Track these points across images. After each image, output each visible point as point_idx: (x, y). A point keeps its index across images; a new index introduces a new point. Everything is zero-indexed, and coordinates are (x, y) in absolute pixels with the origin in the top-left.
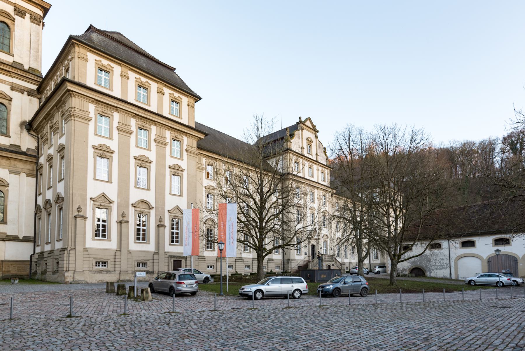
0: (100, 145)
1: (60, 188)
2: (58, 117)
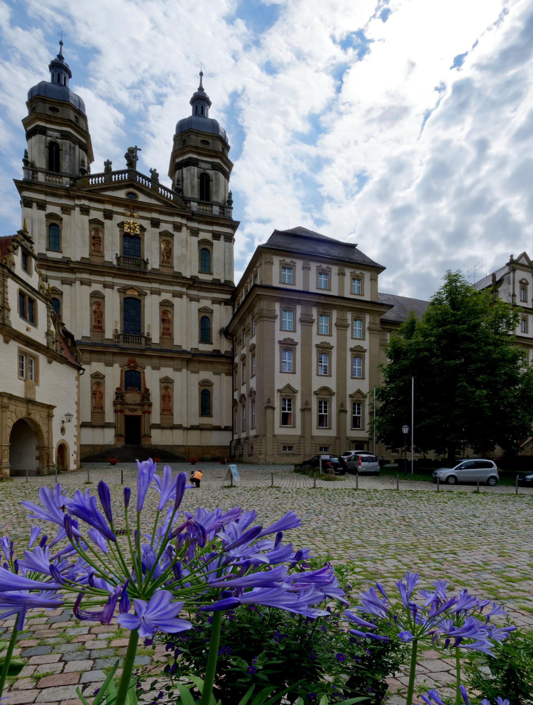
0: (285, 339)
1: (253, 383)
2: (249, 319)
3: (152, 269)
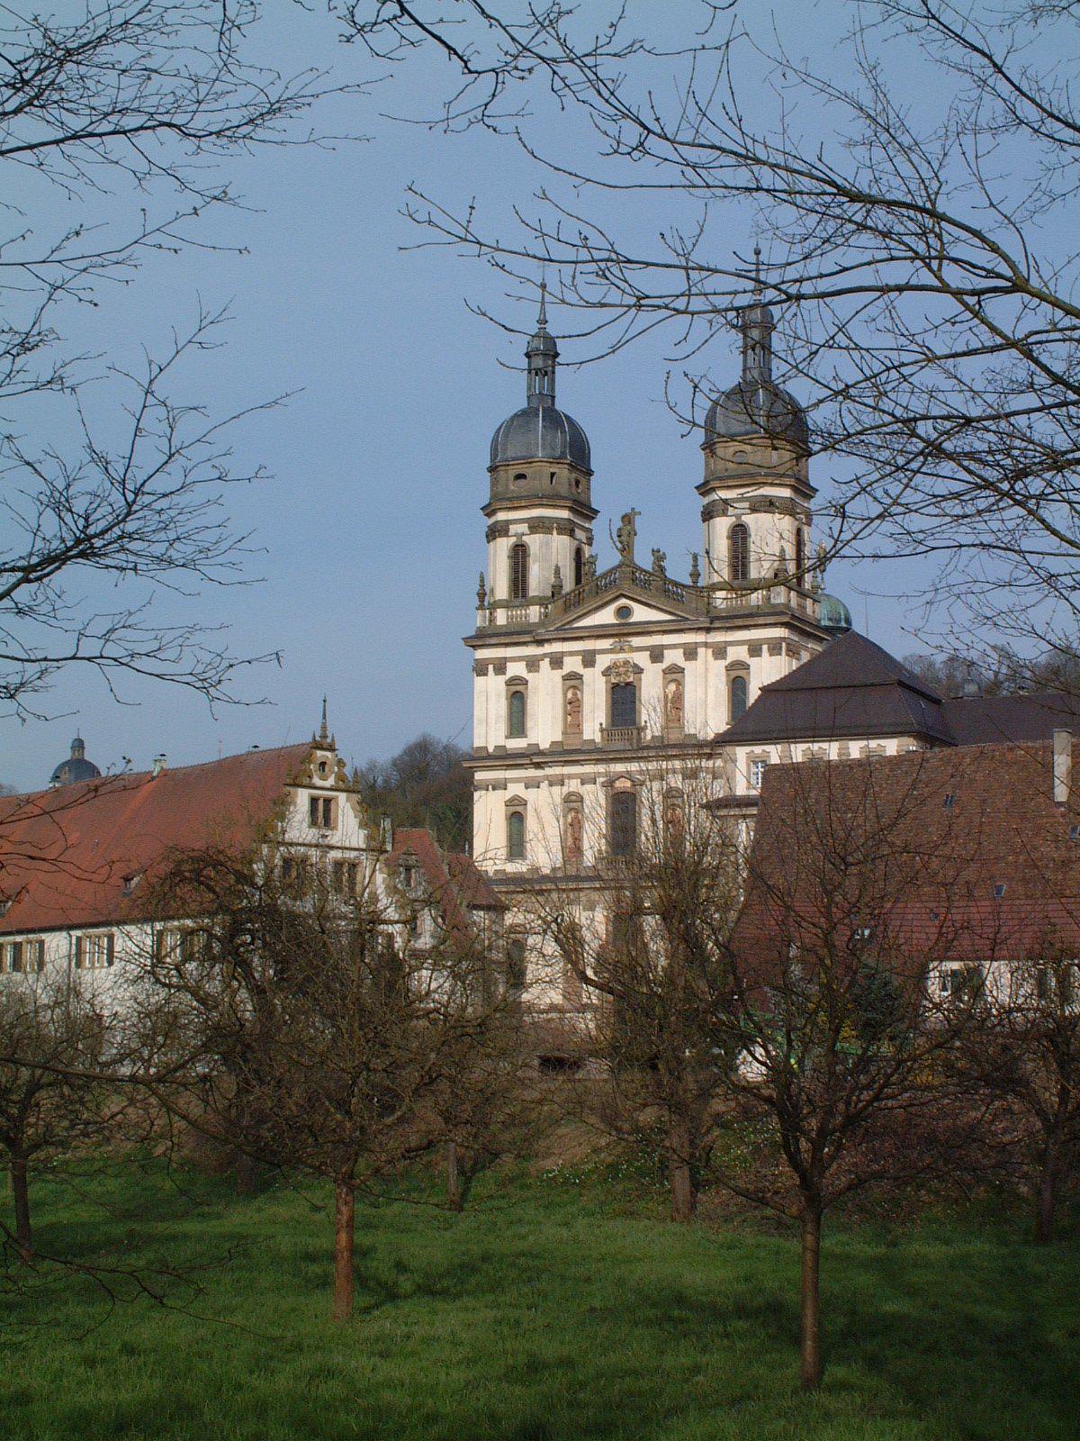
3: (652, 737)
